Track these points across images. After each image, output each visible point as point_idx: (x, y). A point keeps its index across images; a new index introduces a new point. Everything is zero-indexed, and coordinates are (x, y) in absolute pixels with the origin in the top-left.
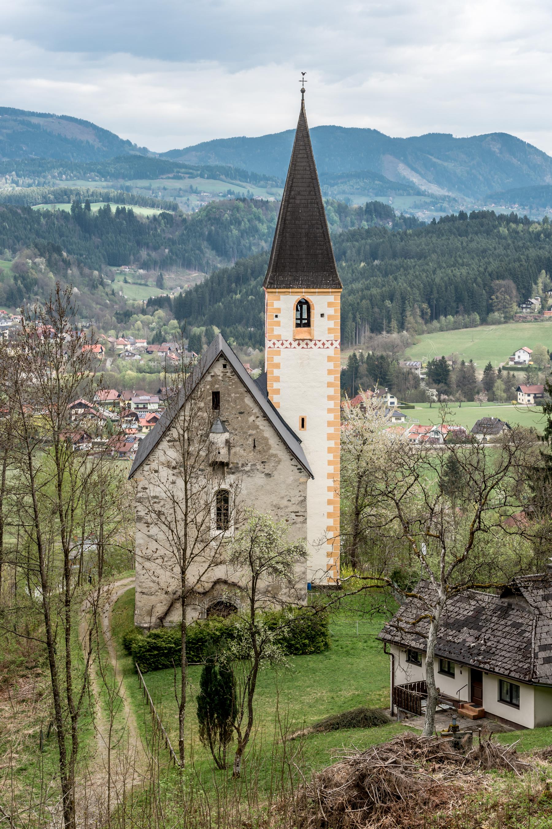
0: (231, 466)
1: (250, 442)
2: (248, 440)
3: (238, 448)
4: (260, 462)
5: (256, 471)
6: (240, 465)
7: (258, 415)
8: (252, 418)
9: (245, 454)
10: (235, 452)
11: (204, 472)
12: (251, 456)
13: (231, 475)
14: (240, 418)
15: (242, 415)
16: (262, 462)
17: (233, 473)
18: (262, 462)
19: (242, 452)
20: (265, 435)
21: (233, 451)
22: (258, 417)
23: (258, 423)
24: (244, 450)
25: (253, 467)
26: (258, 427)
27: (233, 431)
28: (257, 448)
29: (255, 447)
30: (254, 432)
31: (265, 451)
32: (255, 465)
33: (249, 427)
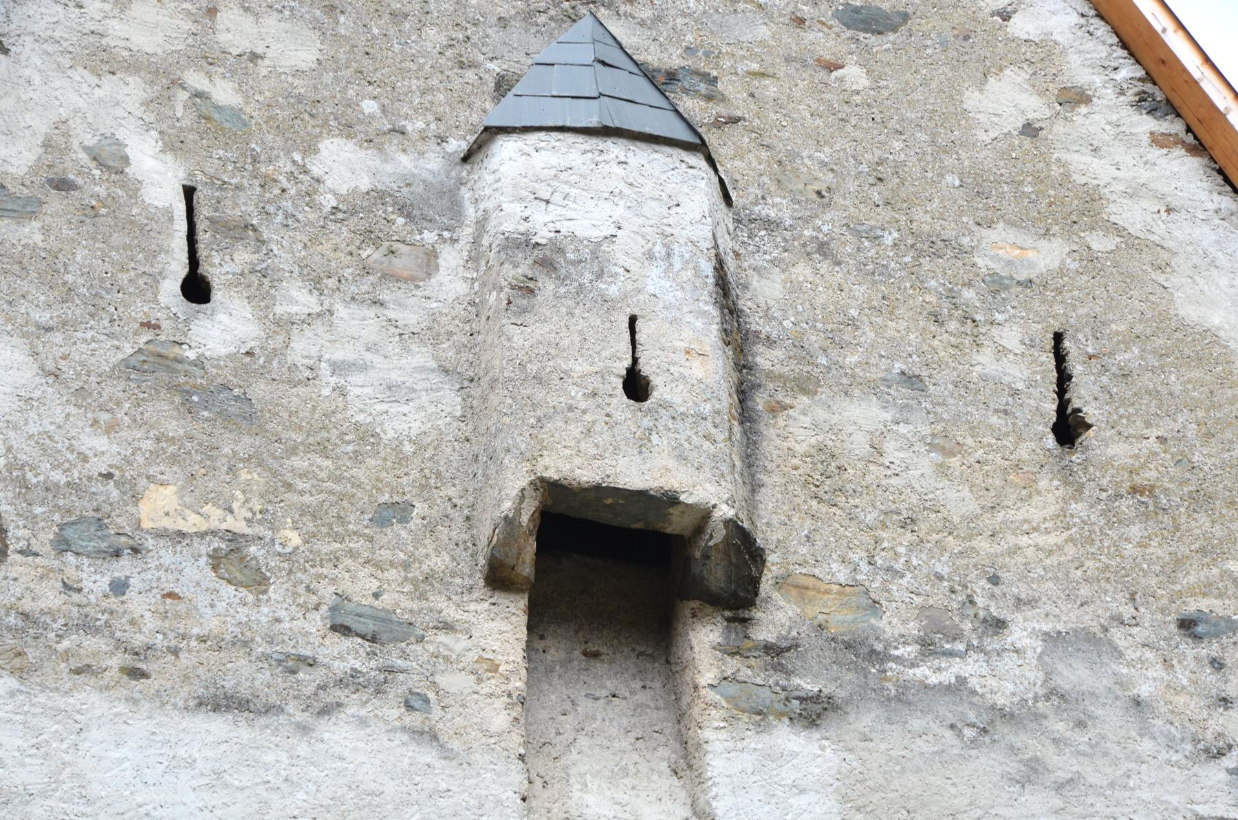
0: (776, 617)
1: (1011, 360)
2: (974, 329)
3: (863, 415)
4: (1154, 623)
5: (1112, 721)
6: (896, 625)
7: (1082, 74)
8: (1005, 101)
9: (959, 501)
10: (826, 457)
11: (412, 660)
12: (1041, 515)
13: (788, 739)
14: (854, 75)
15: (882, 44)
16: (1187, 625)
17: (813, 712)
18: (1187, 625)
19: (914, 470)
20: (1189, 312)
21: (794, 432)
22: (1075, 98)
23: (1088, 168)
24: (942, 444)
25: (1075, 674)
26: (1083, 209)
27: (779, 208)
28: (1105, 445)
29: (1068, 428)
30: (1047, 256)
31: (1200, 499)
32: (1092, 642)
33: (978, 187)
